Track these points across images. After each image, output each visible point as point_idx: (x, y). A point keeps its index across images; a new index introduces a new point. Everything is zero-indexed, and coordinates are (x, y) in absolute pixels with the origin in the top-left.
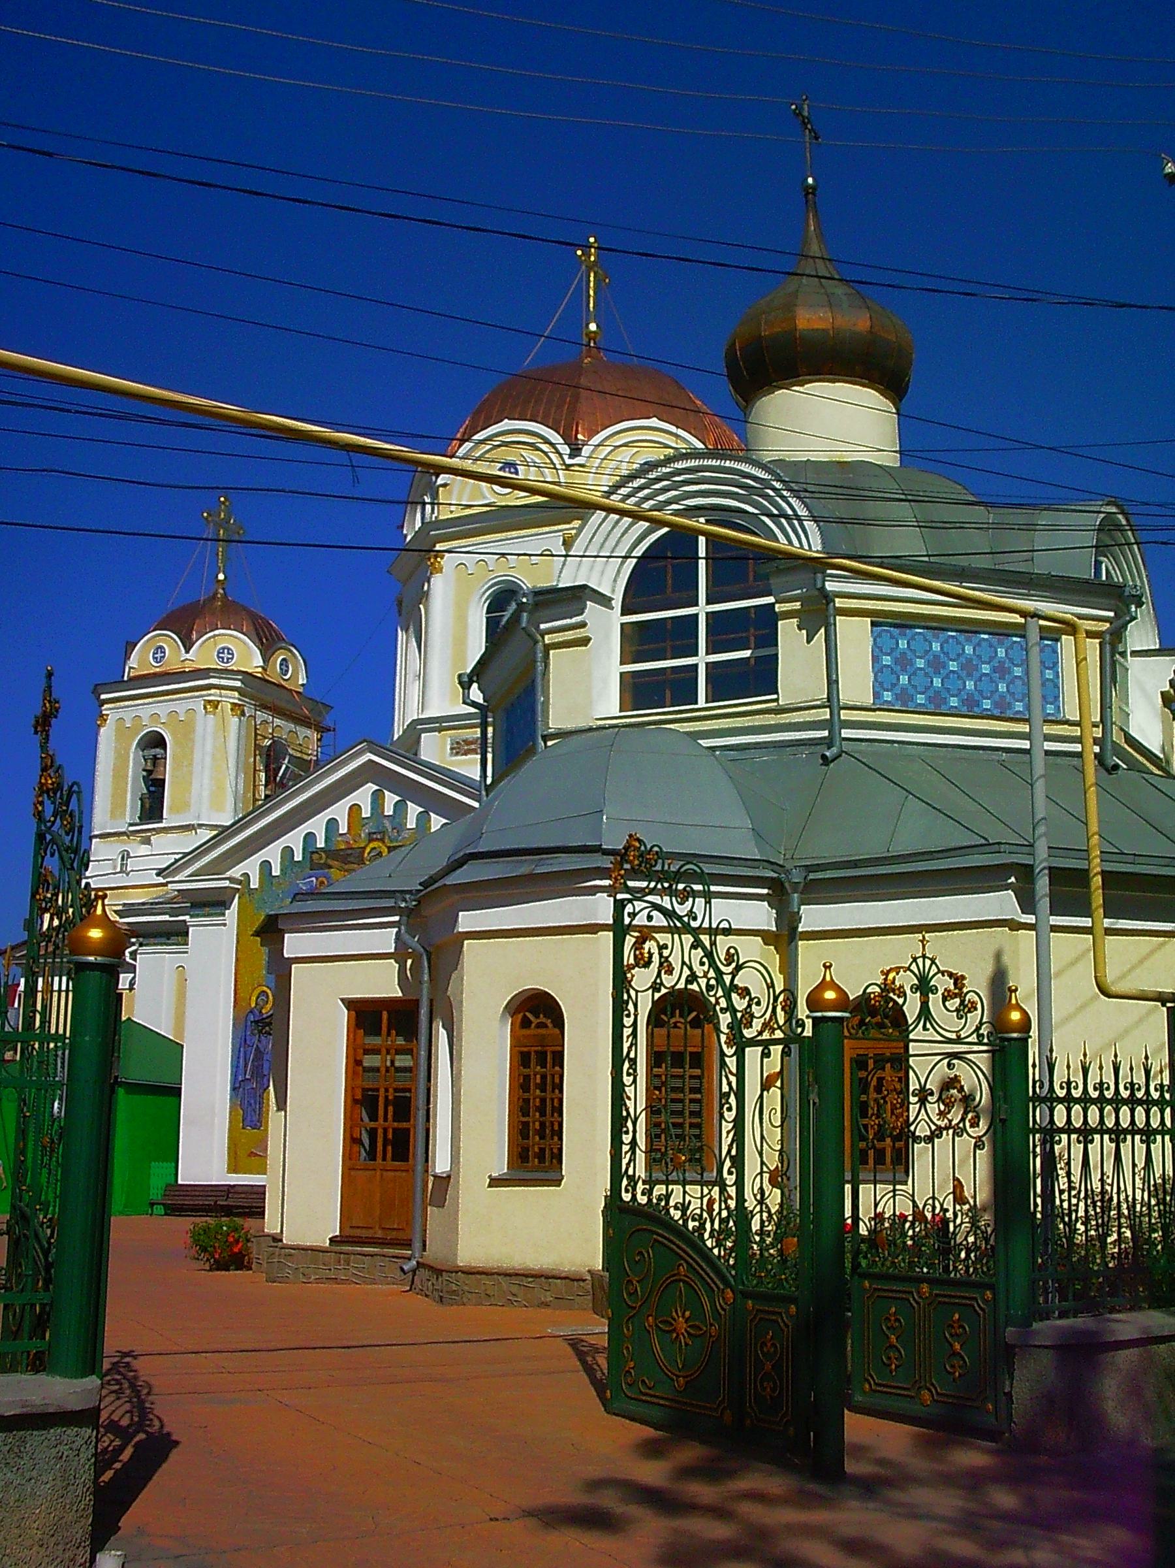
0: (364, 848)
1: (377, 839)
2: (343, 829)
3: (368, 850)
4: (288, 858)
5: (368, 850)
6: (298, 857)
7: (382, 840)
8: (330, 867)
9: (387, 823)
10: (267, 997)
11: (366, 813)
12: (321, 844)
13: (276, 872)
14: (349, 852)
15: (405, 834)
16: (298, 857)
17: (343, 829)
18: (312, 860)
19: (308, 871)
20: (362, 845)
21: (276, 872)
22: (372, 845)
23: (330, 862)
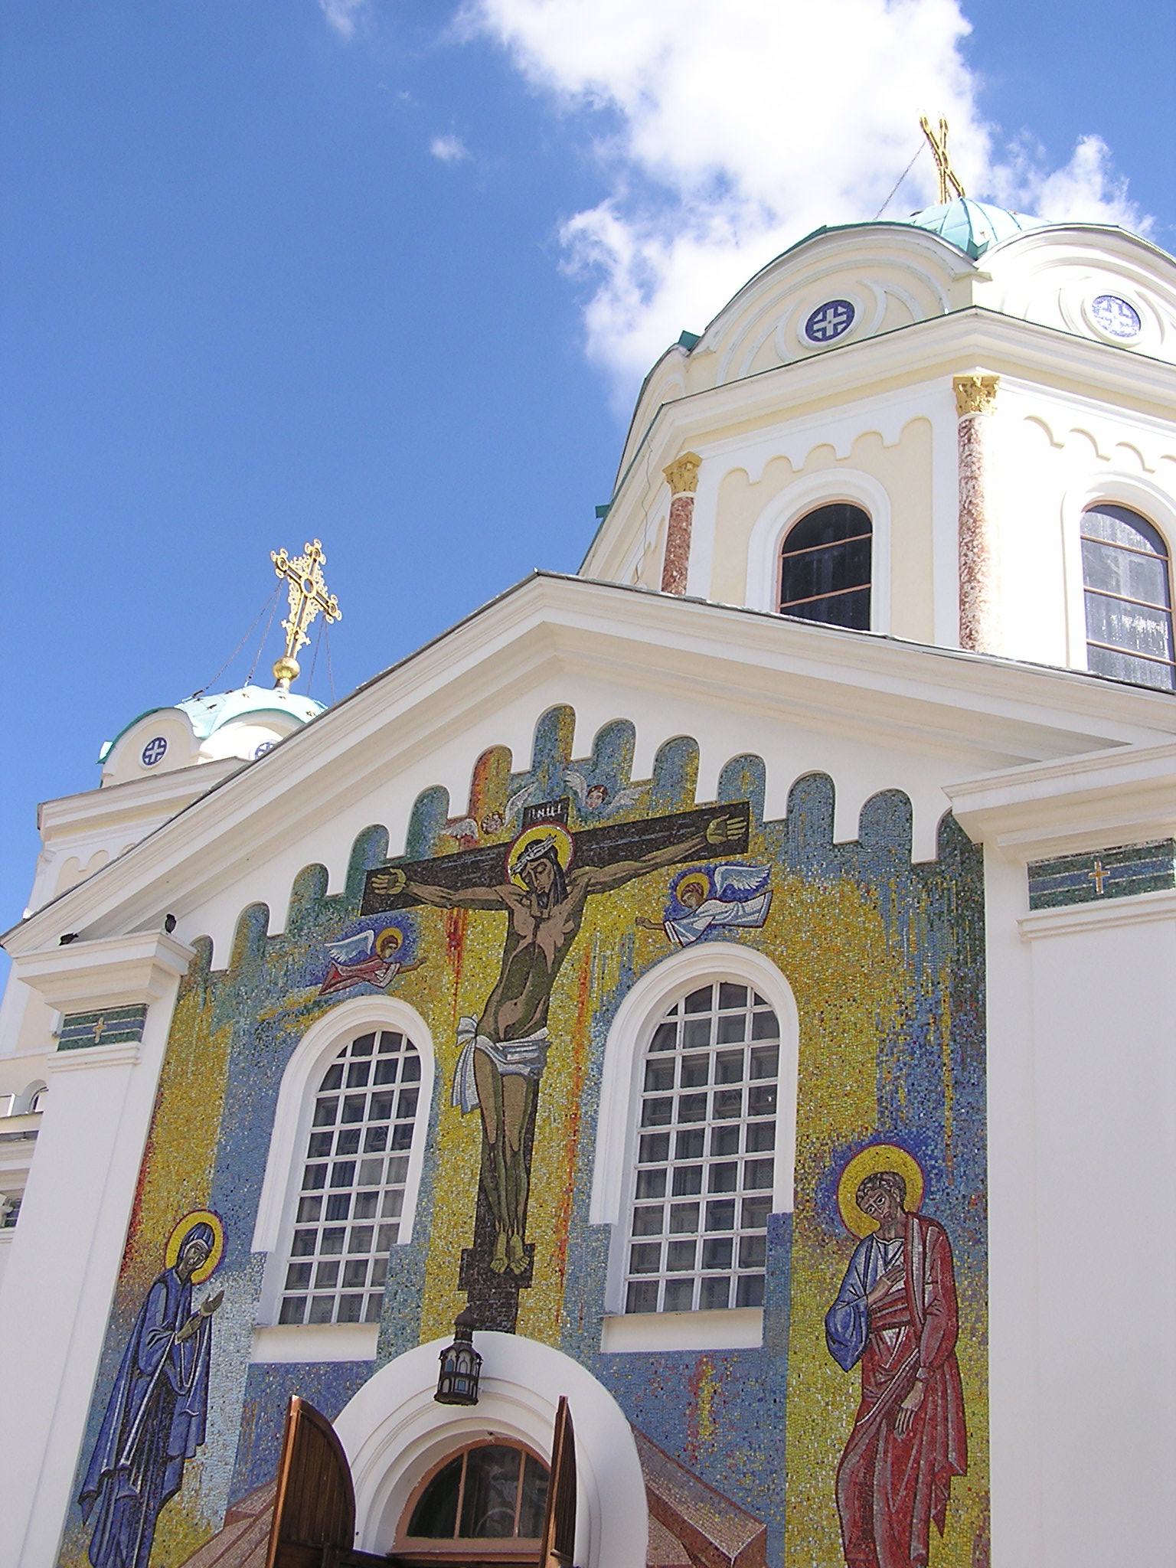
0: (509, 846)
1: (545, 820)
2: (458, 807)
3: (519, 847)
4: (310, 892)
5: (519, 847)
6: (337, 885)
7: (560, 820)
8: (417, 901)
9: (577, 781)
10: (211, 1240)
11: (522, 762)
12: (397, 847)
13: (277, 925)
14: (469, 859)
15: (623, 799)
16: (337, 885)
17: (458, 807)
18: (369, 890)
19: (356, 917)
20: (506, 838)
21: (277, 925)
22: (532, 834)
23: (416, 889)
